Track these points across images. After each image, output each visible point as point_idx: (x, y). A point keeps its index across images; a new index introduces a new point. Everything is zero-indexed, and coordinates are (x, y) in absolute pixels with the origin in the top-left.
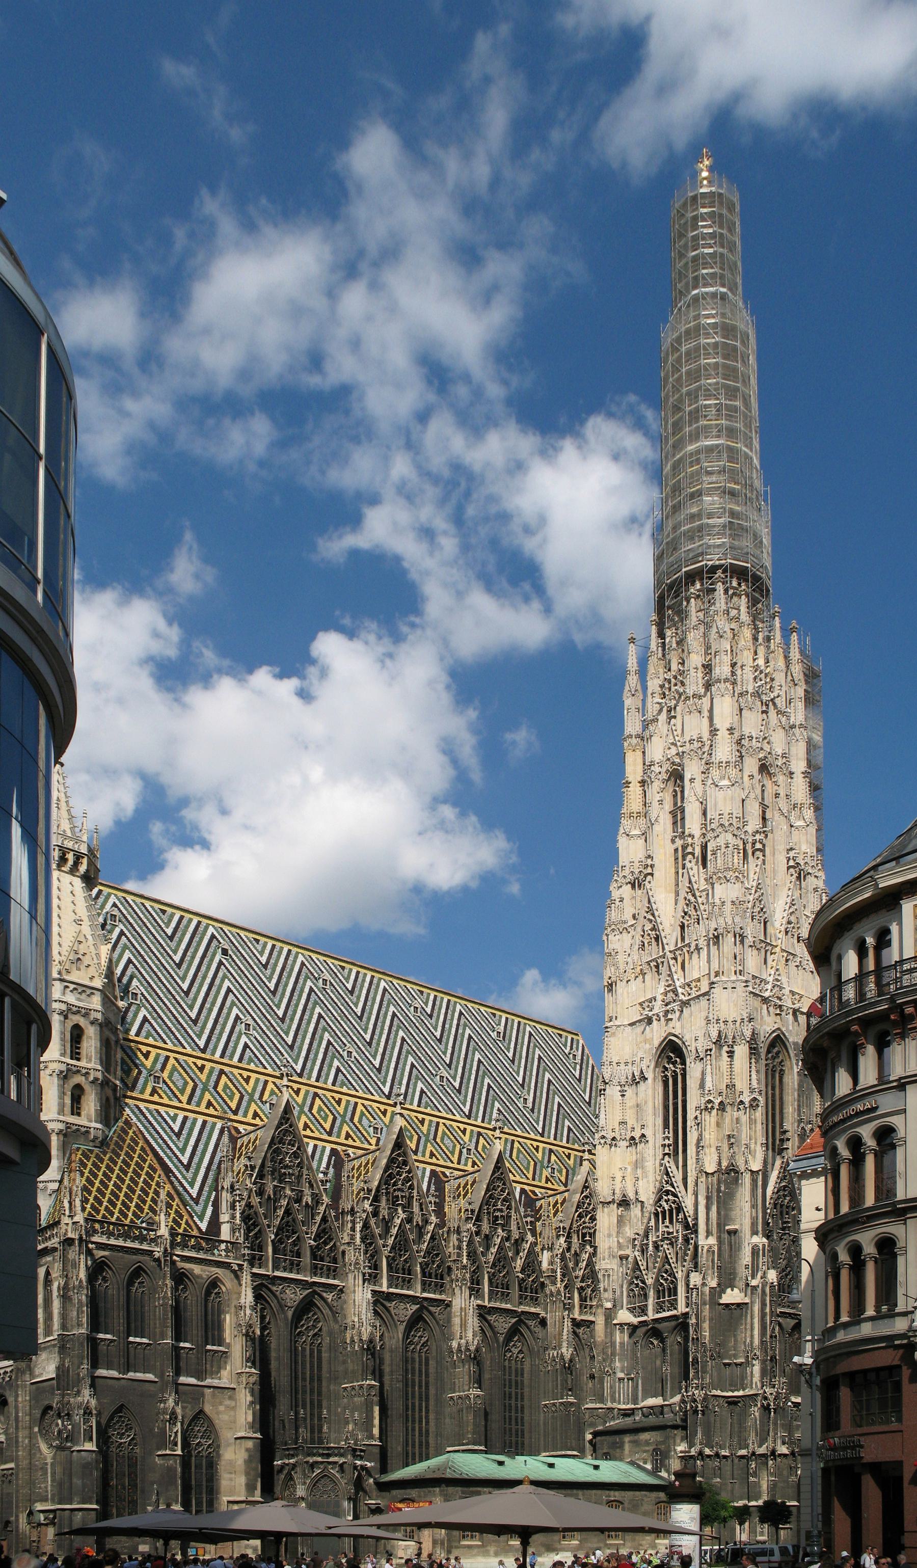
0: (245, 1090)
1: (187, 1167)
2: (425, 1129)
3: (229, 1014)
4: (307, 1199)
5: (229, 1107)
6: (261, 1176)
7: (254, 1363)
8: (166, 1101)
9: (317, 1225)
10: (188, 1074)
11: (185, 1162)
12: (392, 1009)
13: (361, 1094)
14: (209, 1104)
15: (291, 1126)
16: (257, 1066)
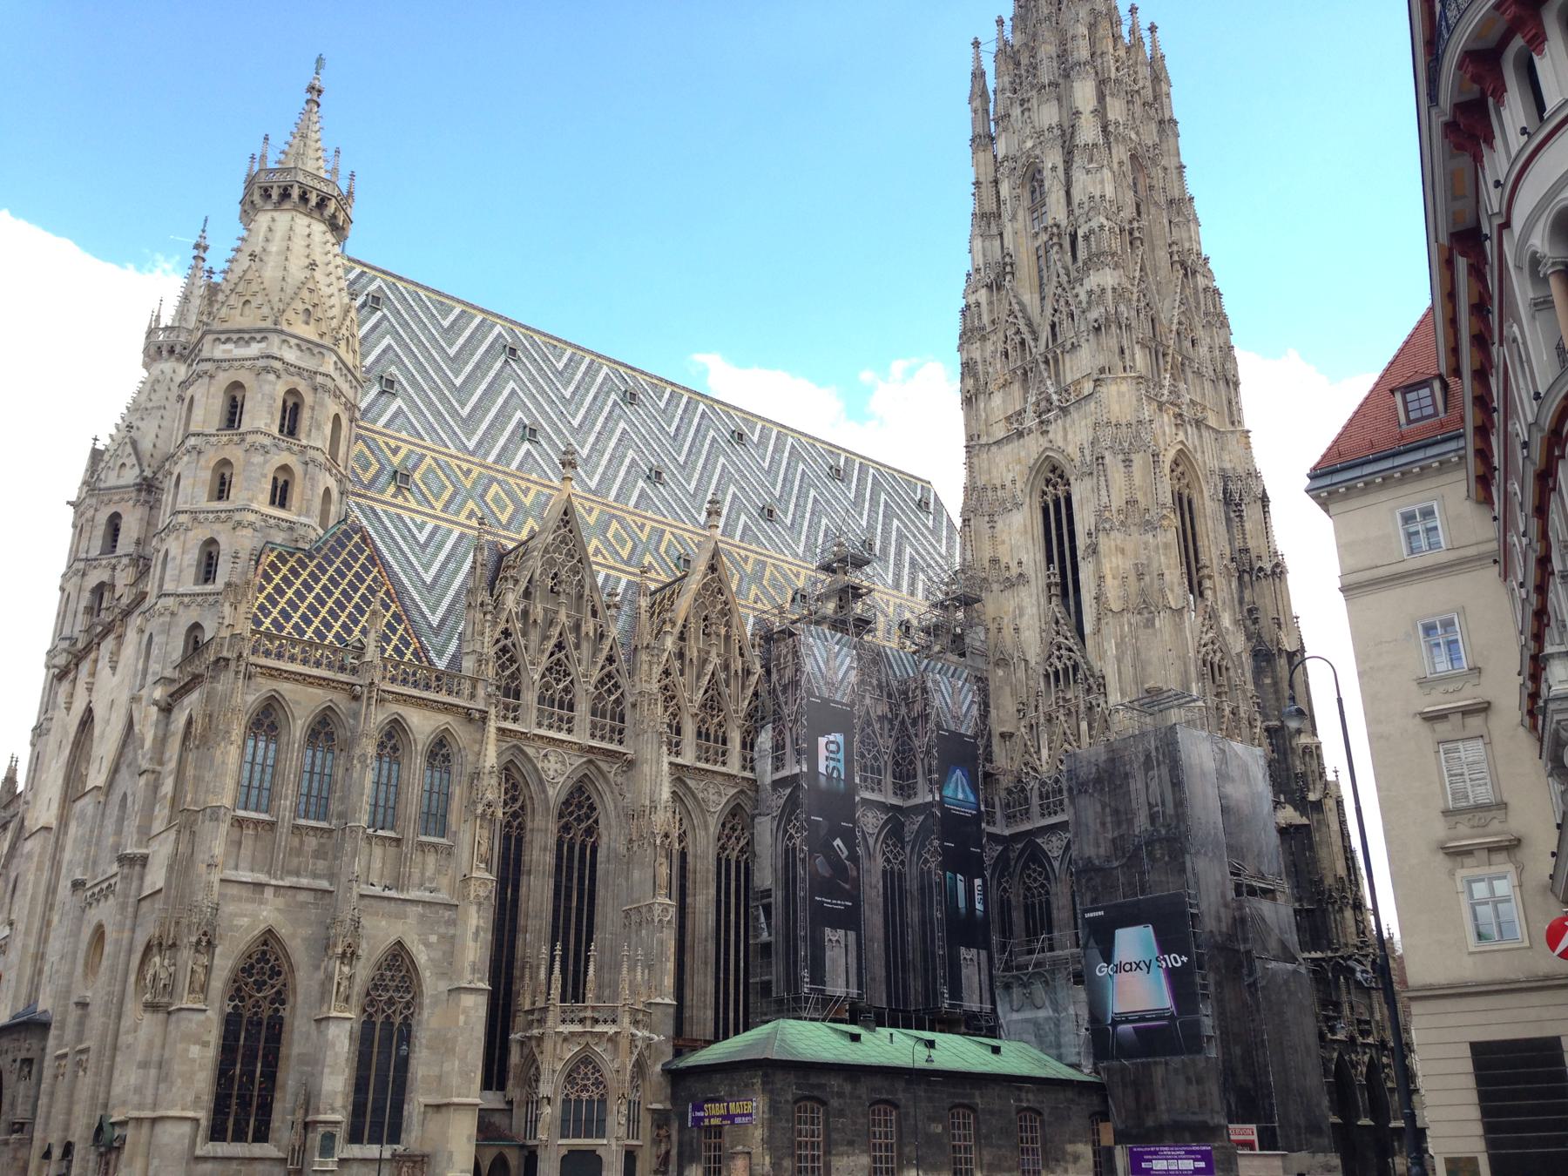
0: (522, 503)
1: (430, 588)
2: (749, 568)
3: (510, 417)
4: (589, 627)
5: (498, 521)
6: (527, 594)
7: (488, 863)
8: (413, 505)
9: (600, 665)
10: (448, 477)
11: (428, 580)
12: (712, 433)
13: (670, 520)
14: (471, 514)
15: (571, 531)
16: (540, 477)
